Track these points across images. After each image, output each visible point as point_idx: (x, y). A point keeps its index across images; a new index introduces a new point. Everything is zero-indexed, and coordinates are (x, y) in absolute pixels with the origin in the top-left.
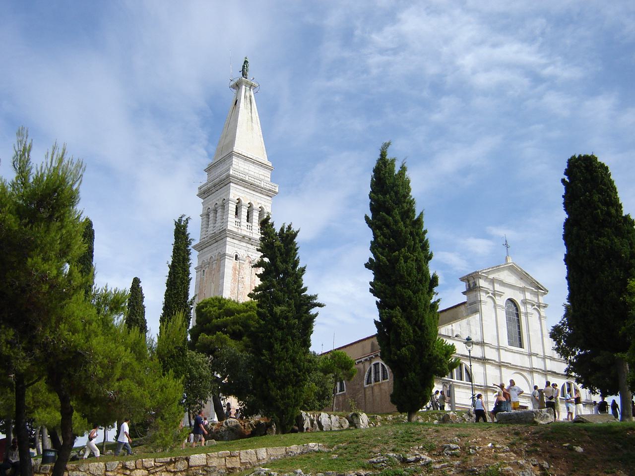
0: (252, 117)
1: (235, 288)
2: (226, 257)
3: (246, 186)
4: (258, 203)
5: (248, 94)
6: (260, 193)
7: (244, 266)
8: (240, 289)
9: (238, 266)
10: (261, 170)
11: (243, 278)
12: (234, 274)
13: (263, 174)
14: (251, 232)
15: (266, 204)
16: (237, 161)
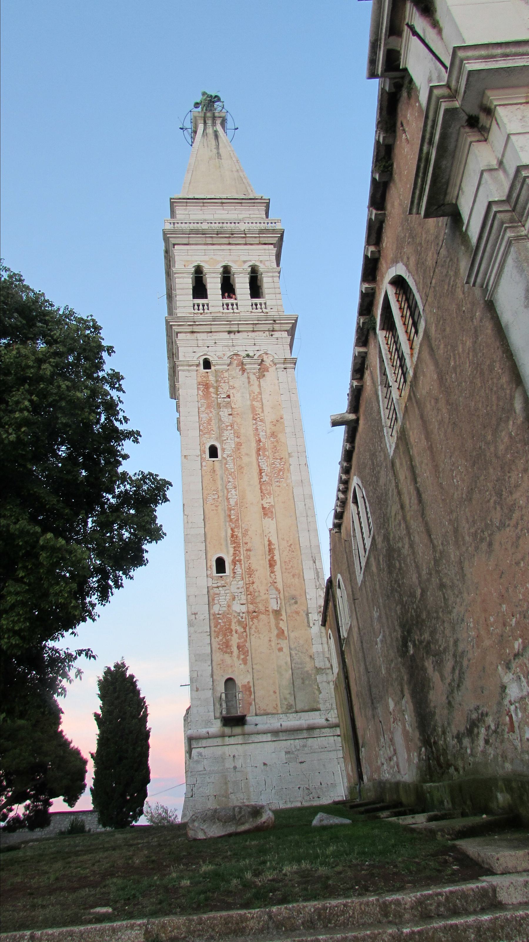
0: (218, 153)
1: (210, 420)
2: (179, 368)
3: (209, 241)
4: (245, 262)
5: (210, 131)
6: (246, 244)
7: (226, 374)
8: (227, 420)
9: (212, 379)
10: (243, 212)
11: (229, 396)
12: (206, 394)
13: (248, 216)
14: (236, 311)
15: (261, 258)
16: (186, 212)
